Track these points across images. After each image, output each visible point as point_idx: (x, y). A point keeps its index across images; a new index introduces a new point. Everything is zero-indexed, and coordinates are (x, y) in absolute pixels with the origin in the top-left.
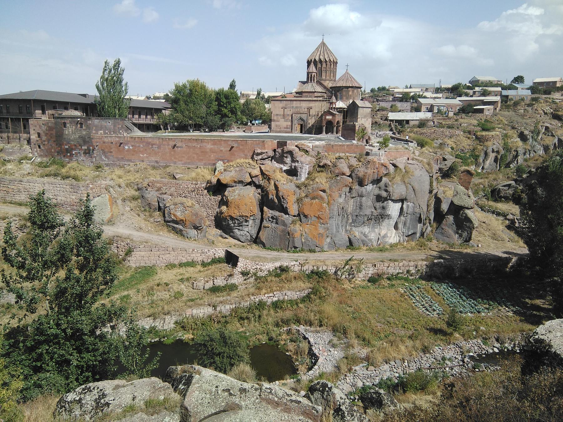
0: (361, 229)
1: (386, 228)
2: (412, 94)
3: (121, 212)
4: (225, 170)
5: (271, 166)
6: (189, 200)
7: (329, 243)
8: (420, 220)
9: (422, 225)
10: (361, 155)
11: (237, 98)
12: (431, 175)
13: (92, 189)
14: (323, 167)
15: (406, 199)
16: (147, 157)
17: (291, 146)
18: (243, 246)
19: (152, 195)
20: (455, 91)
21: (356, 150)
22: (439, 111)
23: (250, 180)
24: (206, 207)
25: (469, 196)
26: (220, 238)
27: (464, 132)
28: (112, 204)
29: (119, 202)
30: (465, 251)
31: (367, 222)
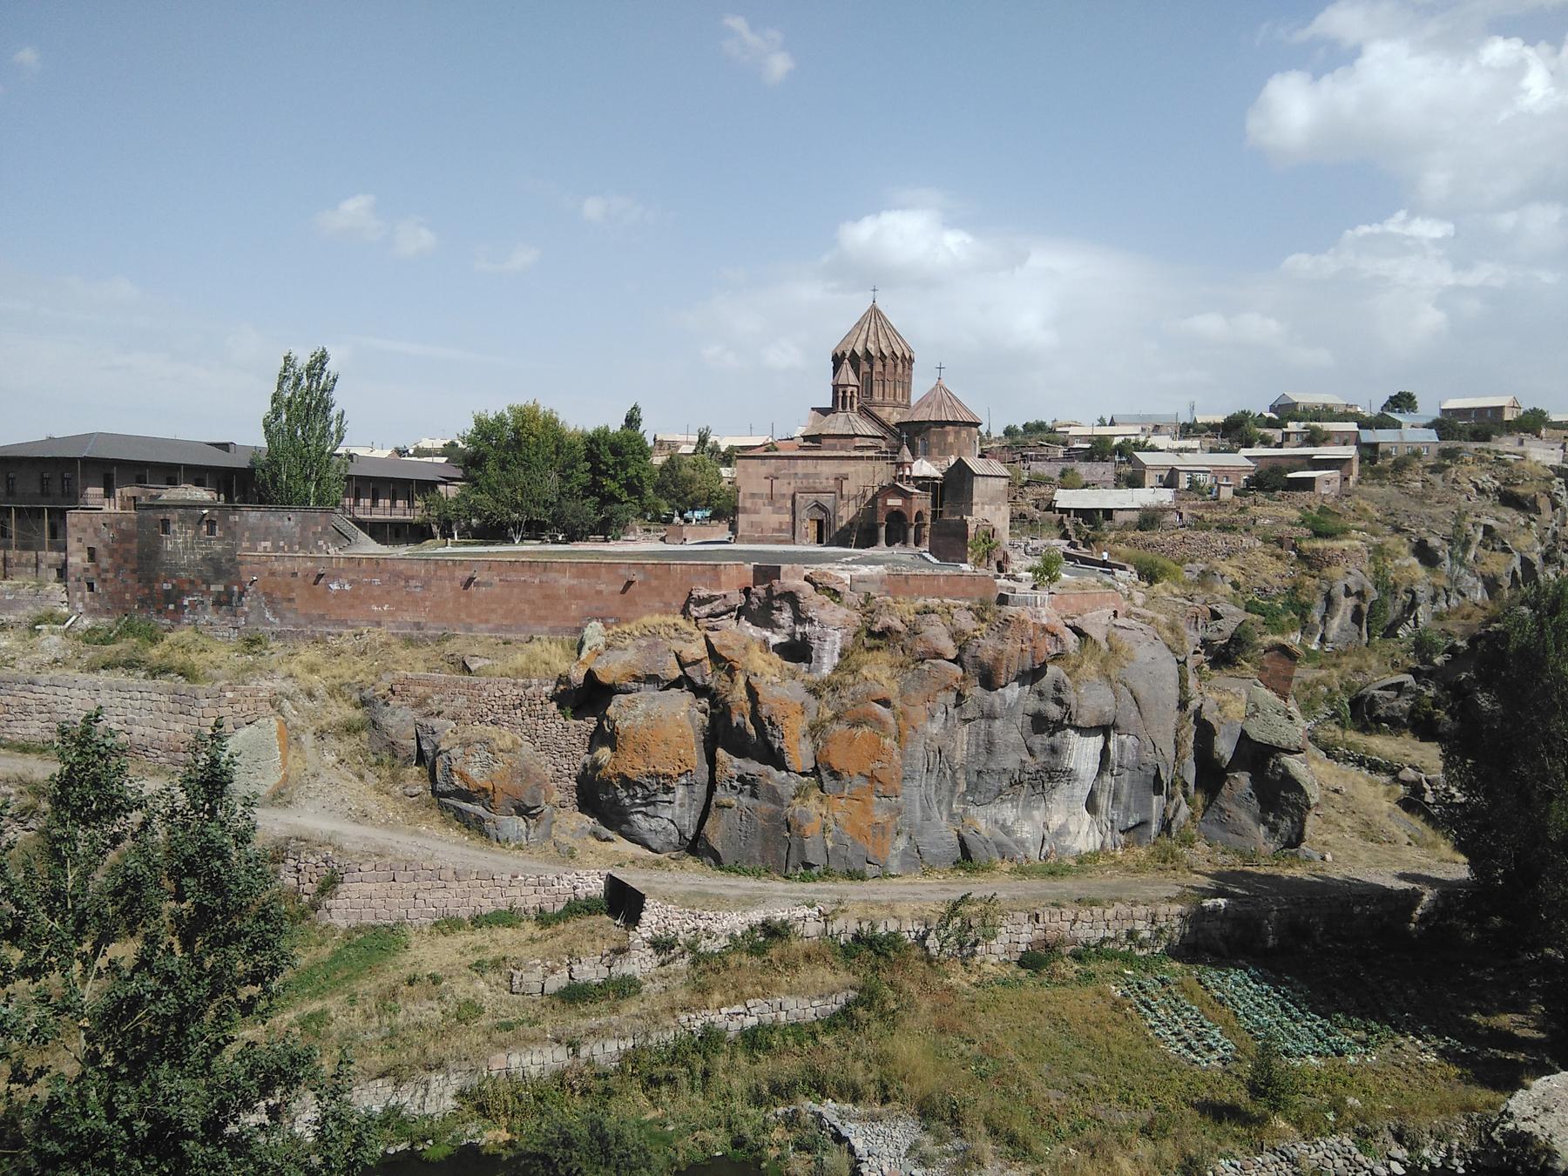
2: (1117, 441)
3: (311, 770)
4: (608, 646)
5: (738, 635)
7: (905, 852)
8: (1157, 786)
9: (1163, 798)
11: (645, 452)
12: (1181, 659)
13: (232, 703)
15: (1115, 726)
16: (390, 614)
17: (792, 579)
18: (658, 864)
19: (400, 720)
20: (1235, 431)
21: (970, 589)
22: (1194, 486)
23: (678, 673)
24: (553, 751)
25: (1290, 718)
26: (593, 841)
27: (1266, 541)
28: (285, 747)
29: (308, 739)
31: (1010, 791)
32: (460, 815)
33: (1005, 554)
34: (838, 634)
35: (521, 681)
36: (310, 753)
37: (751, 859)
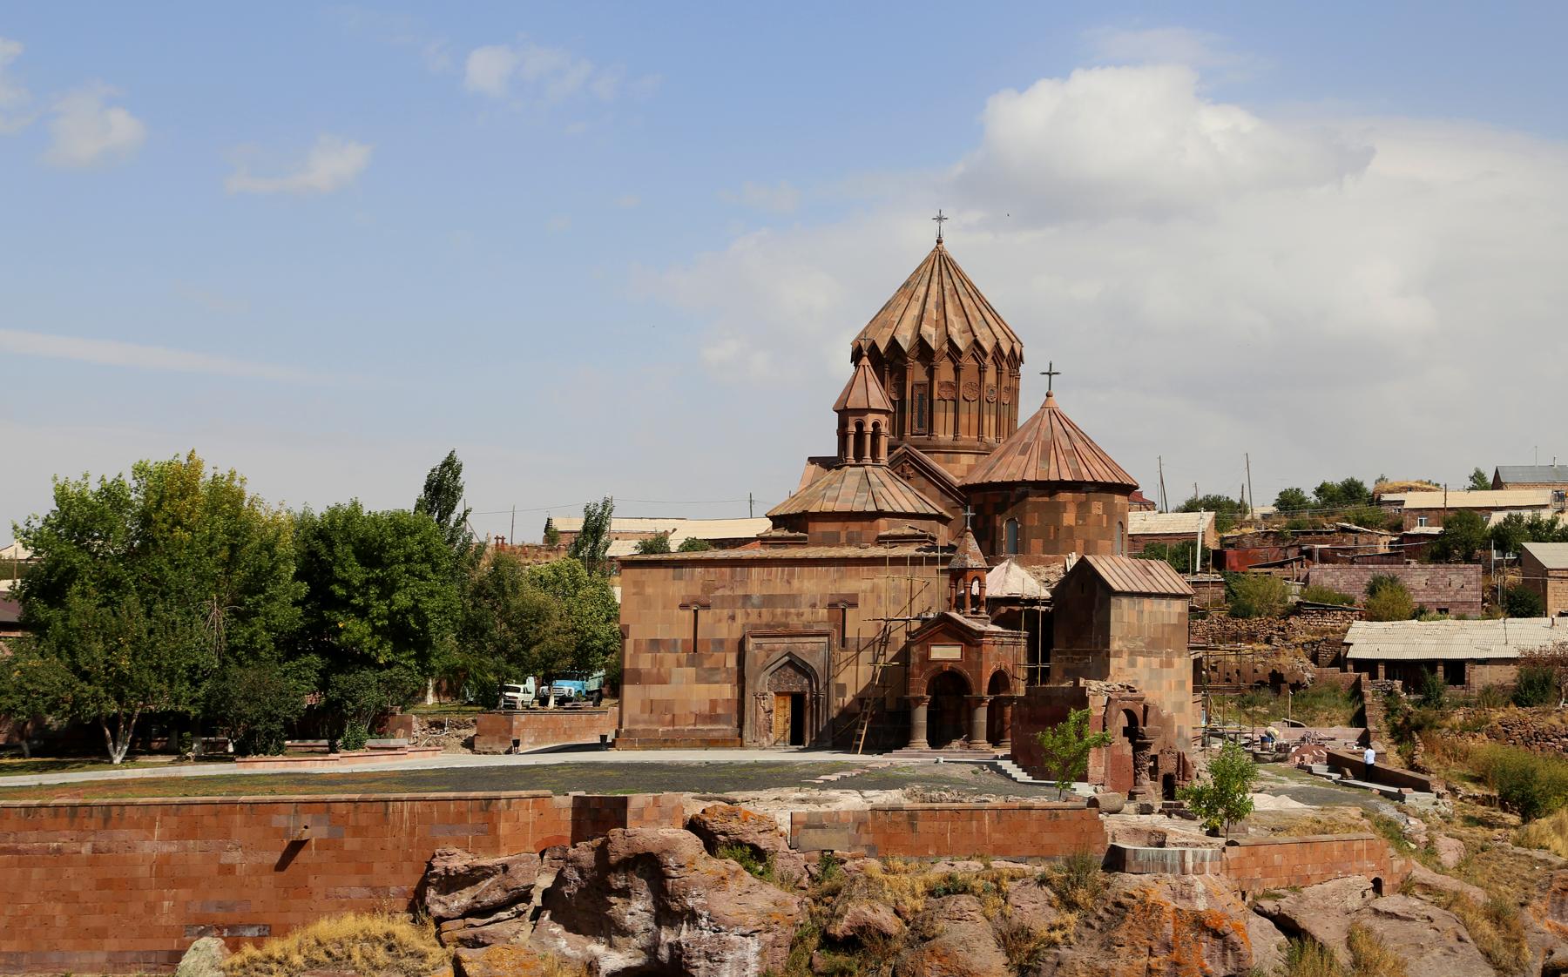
10: (1077, 868)
17: (656, 825)
21: (1048, 838)
33: (1181, 759)
34: (753, 945)
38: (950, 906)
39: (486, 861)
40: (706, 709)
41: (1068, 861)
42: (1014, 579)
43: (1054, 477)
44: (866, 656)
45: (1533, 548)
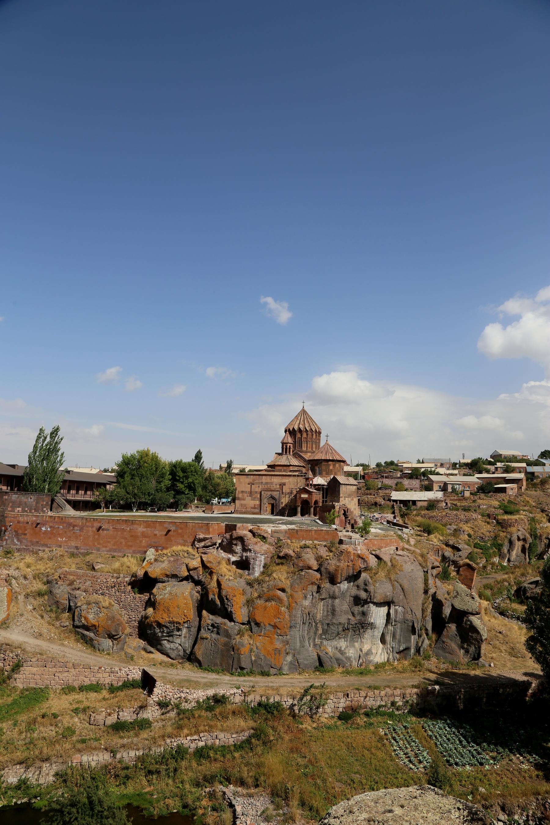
0: (336, 643)
1: (369, 641)
4: (156, 560)
5: (216, 556)
6: (106, 598)
7: (291, 663)
8: (413, 631)
9: (416, 636)
10: (332, 543)
12: (426, 570)
14: (283, 559)
17: (243, 531)
18: (172, 665)
19: (62, 591)
21: (326, 537)
23: (186, 574)
24: (127, 609)
26: (143, 653)
28: (10, 601)
29: (21, 598)
30: (472, 673)
31: (343, 633)
32: (83, 637)
33: (355, 520)
34: (263, 557)
35: (115, 575)
36: (21, 604)
37: (215, 665)
38: (305, 550)
39: (207, 536)
40: (253, 506)
41: (331, 542)
42: (319, 480)
43: (328, 458)
44: (287, 496)
45: (430, 476)
